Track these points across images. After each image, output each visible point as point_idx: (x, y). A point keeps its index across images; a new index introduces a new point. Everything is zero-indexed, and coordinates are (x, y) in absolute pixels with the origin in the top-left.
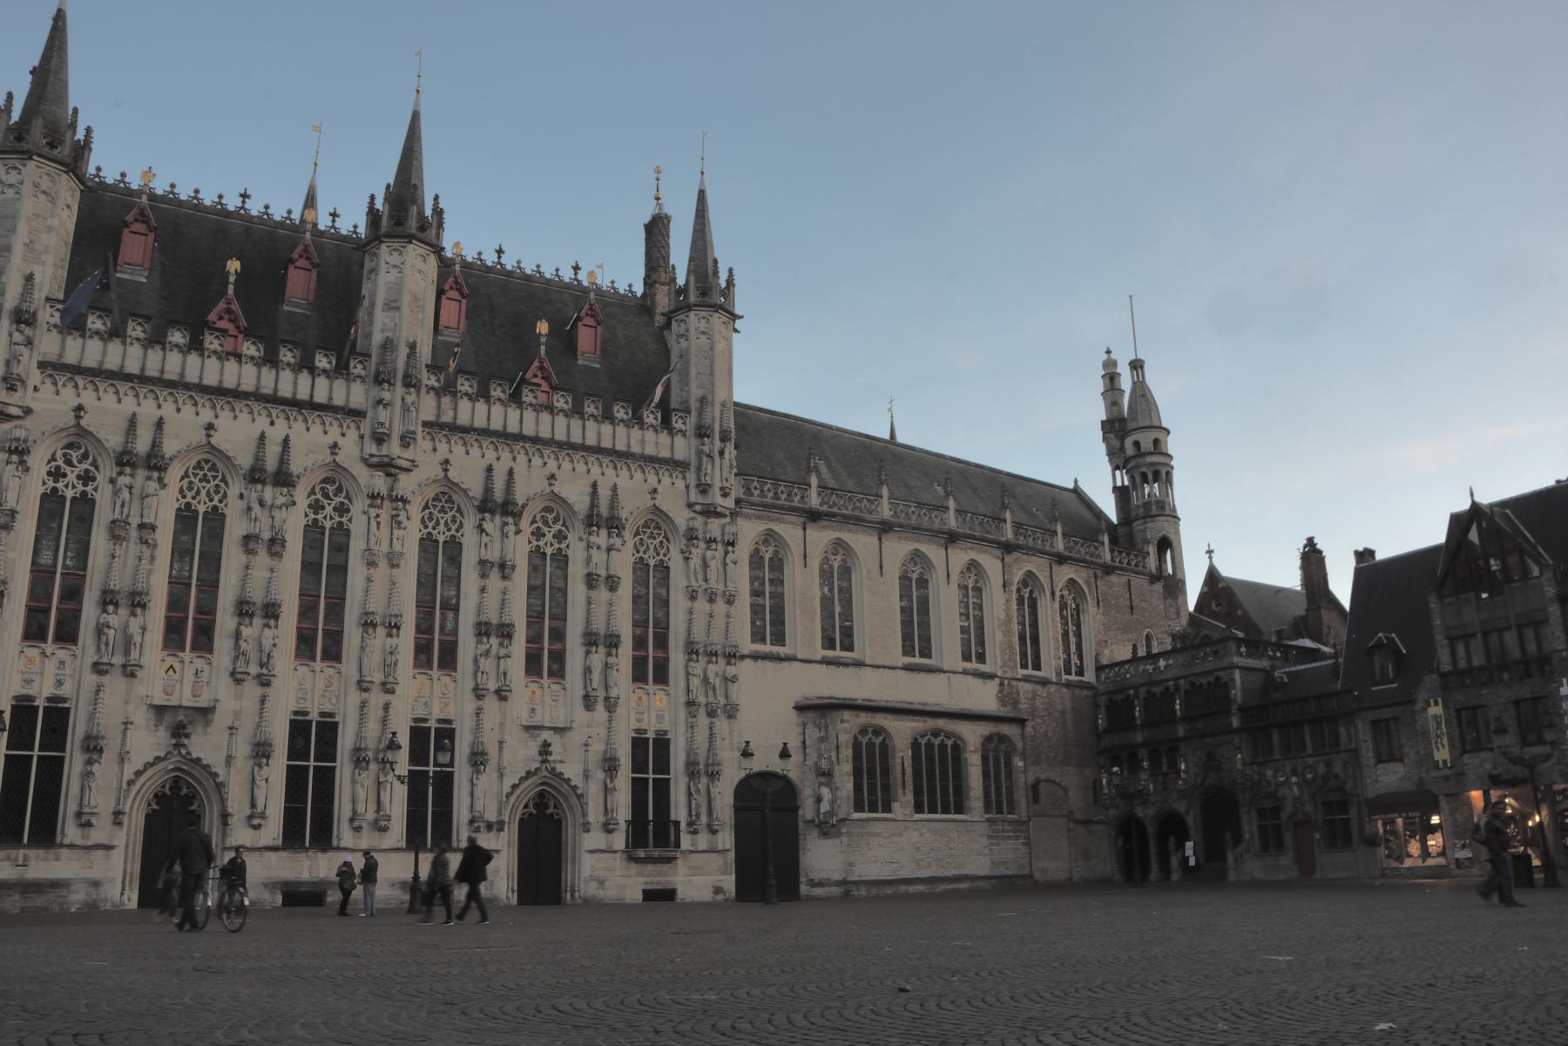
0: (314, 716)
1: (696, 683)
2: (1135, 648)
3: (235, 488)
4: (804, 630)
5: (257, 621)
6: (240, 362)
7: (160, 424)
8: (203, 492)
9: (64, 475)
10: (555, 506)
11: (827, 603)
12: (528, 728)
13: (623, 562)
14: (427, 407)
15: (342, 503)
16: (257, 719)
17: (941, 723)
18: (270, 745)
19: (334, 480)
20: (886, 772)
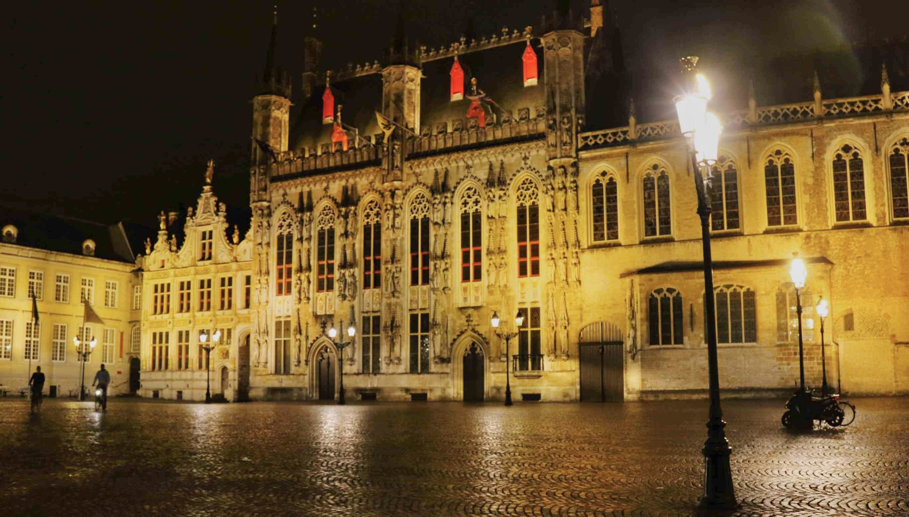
11: (649, 205)
12: (461, 309)
20: (679, 316)
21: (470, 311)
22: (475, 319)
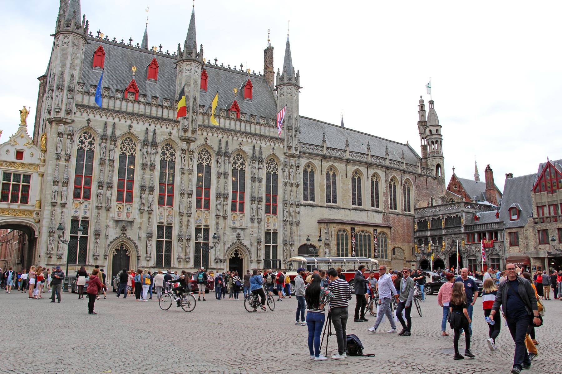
0: (165, 224)
1: (286, 214)
2: (428, 203)
3: (138, 147)
4: (320, 195)
5: (147, 192)
6: (139, 103)
7: (114, 125)
8: (128, 149)
9: (84, 143)
10: (240, 154)
11: (328, 187)
13: (263, 174)
15: (172, 152)
16: (147, 225)
18: (152, 234)
19: (169, 144)
22: (242, 235)
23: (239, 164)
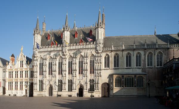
14: (68, 48)
17: (130, 75)
21: (80, 80)
23: (81, 59)
